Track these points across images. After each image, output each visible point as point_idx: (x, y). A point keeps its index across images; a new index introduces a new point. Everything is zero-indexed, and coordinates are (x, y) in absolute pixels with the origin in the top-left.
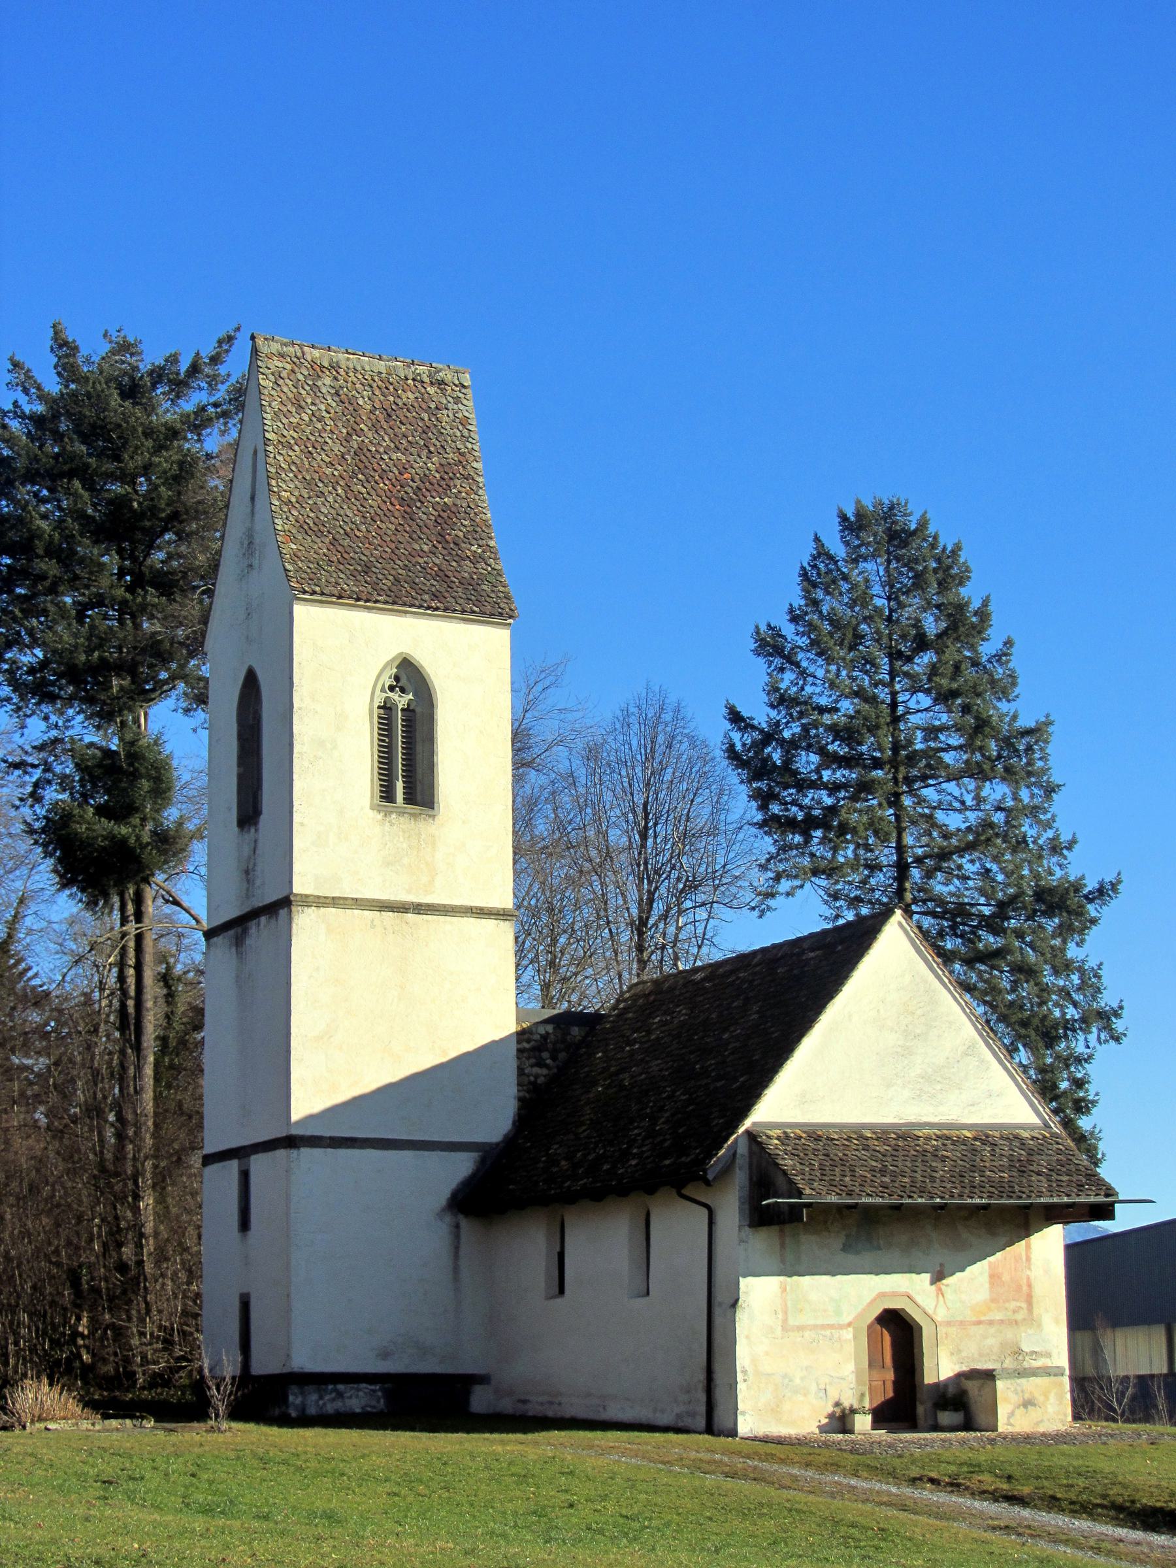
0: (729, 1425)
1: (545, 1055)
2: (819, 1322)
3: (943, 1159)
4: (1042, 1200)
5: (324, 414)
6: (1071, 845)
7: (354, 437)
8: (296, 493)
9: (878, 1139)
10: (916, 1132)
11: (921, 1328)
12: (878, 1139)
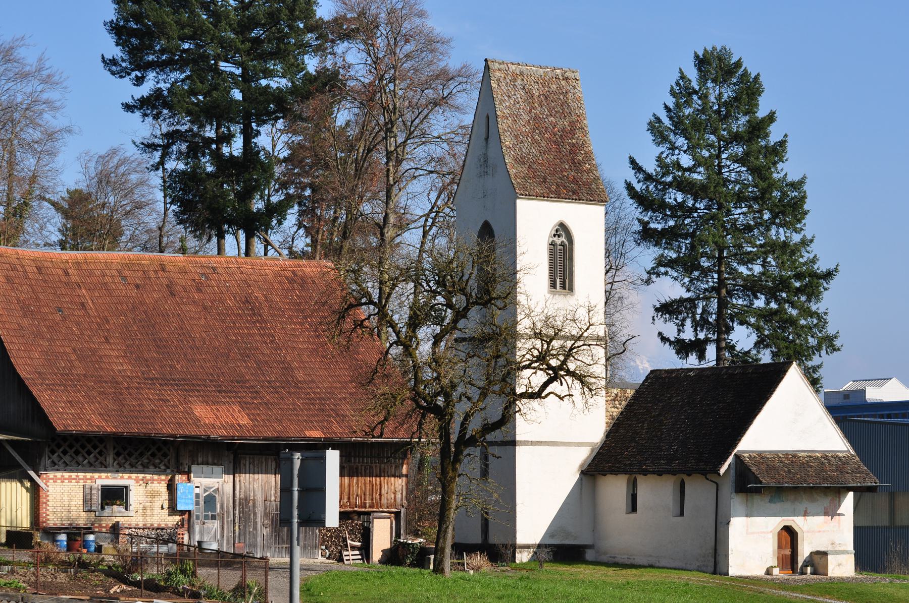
0: (724, 571)
1: (617, 402)
3: (811, 466)
4: (850, 485)
5: (520, 100)
6: (812, 241)
7: (533, 110)
8: (512, 143)
9: (785, 458)
10: (799, 454)
11: (797, 533)
12: (785, 458)
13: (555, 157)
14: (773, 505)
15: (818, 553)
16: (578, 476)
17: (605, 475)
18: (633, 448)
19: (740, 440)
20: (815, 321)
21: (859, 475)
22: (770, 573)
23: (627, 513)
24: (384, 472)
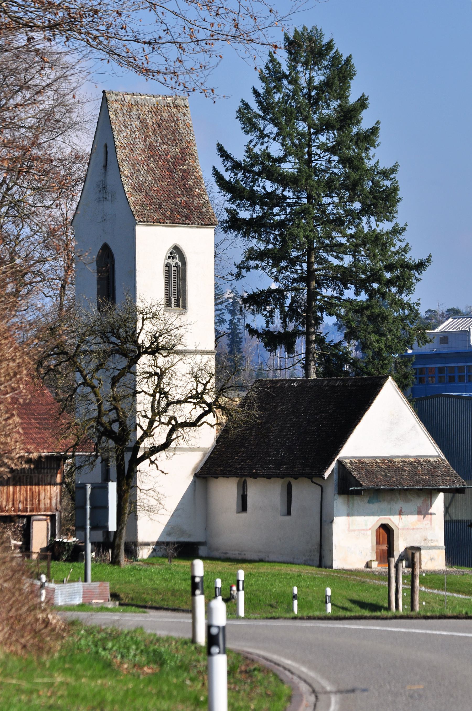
0: (329, 564)
3: (405, 471)
5: (135, 129)
6: (404, 229)
7: (148, 139)
9: (382, 463)
11: (393, 531)
12: (382, 463)
13: (169, 184)
14: (371, 505)
15: (412, 548)
16: (191, 478)
17: (217, 478)
18: (243, 454)
19: (342, 447)
20: (407, 312)
21: (448, 478)
22: (369, 565)
23: (238, 512)
24: (42, 481)
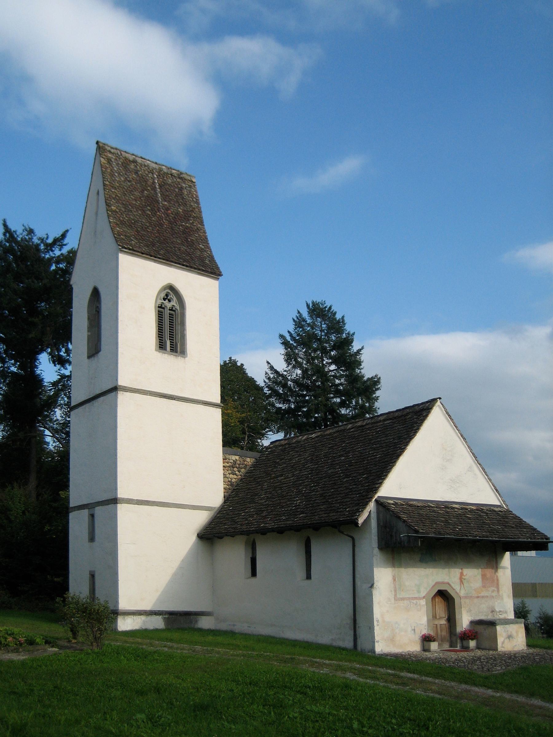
2: (411, 596)
19: (381, 483)
